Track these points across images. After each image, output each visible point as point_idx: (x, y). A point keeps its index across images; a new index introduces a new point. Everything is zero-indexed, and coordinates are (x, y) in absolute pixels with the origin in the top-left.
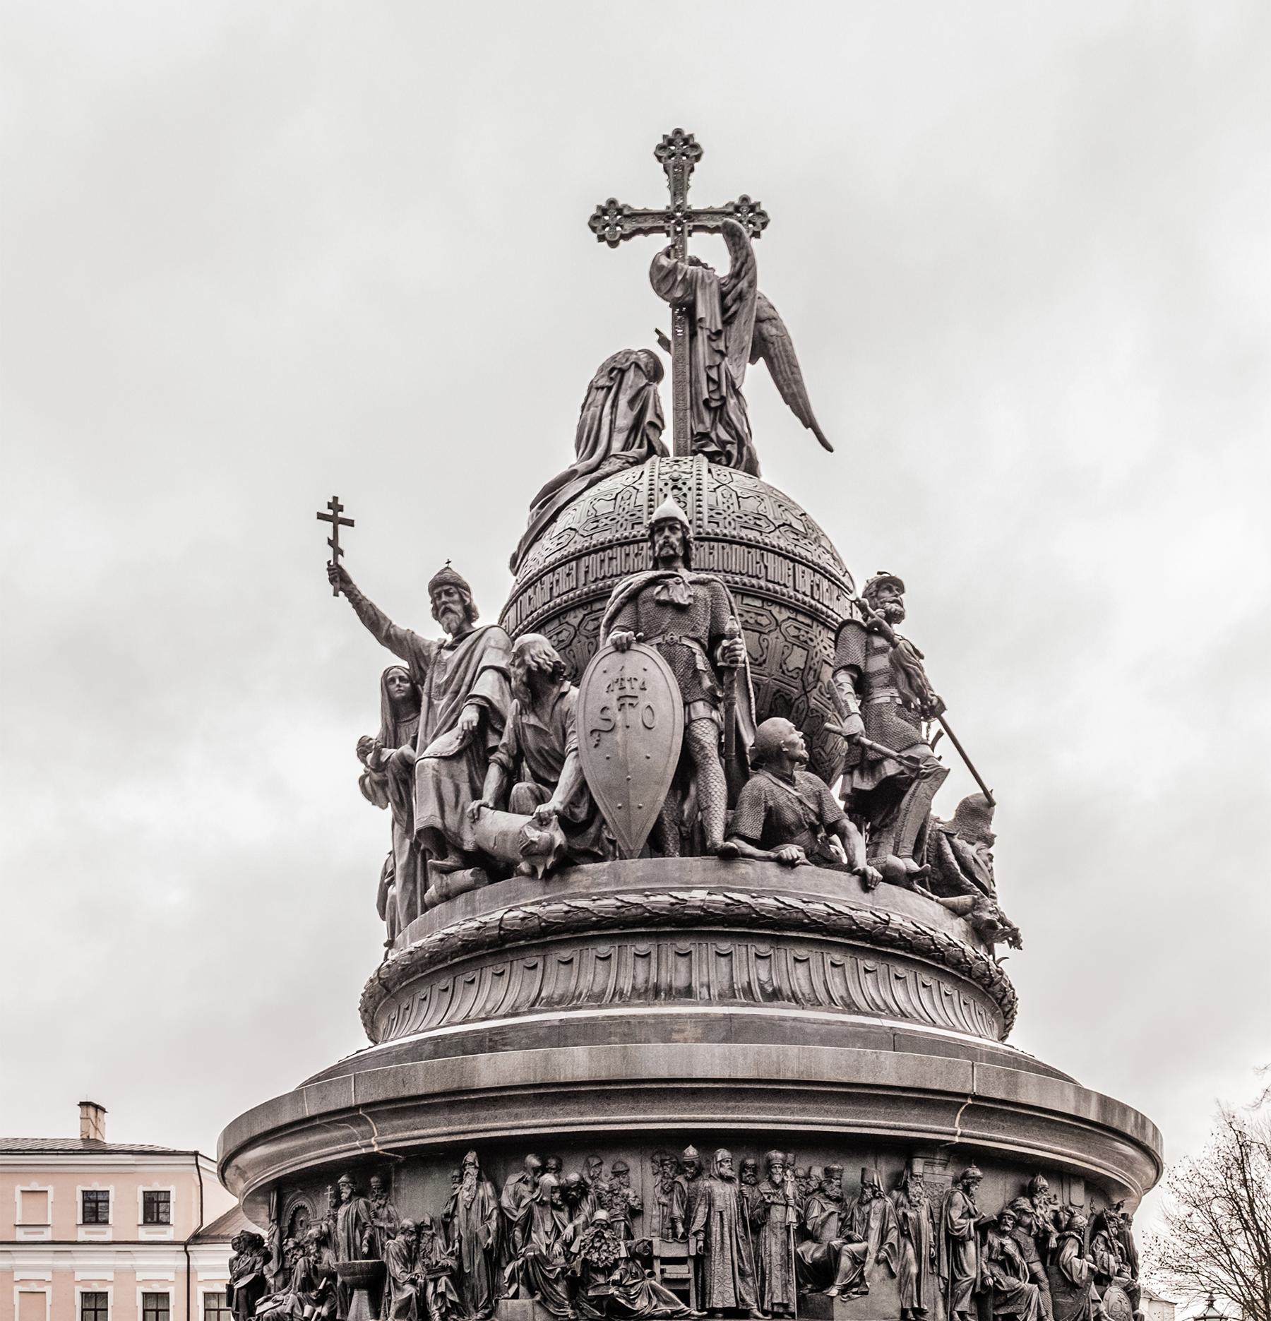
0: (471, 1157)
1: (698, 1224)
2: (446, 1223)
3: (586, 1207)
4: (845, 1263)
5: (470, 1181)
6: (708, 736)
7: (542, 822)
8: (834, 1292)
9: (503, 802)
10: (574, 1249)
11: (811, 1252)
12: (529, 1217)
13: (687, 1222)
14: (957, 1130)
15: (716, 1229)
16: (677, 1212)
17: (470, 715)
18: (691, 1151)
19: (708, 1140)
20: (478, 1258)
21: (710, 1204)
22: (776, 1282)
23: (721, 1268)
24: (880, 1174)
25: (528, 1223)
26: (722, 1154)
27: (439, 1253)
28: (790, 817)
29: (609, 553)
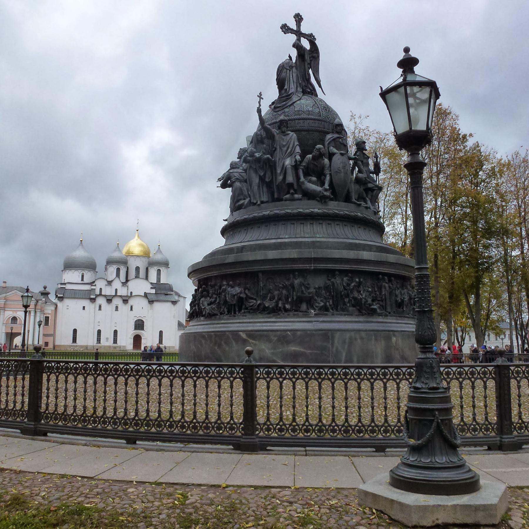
1: (384, 293)
7: (326, 190)
16: (376, 289)
17: (298, 158)
18: (381, 276)
19: (384, 274)
25: (352, 291)
26: (386, 277)
29: (315, 121)
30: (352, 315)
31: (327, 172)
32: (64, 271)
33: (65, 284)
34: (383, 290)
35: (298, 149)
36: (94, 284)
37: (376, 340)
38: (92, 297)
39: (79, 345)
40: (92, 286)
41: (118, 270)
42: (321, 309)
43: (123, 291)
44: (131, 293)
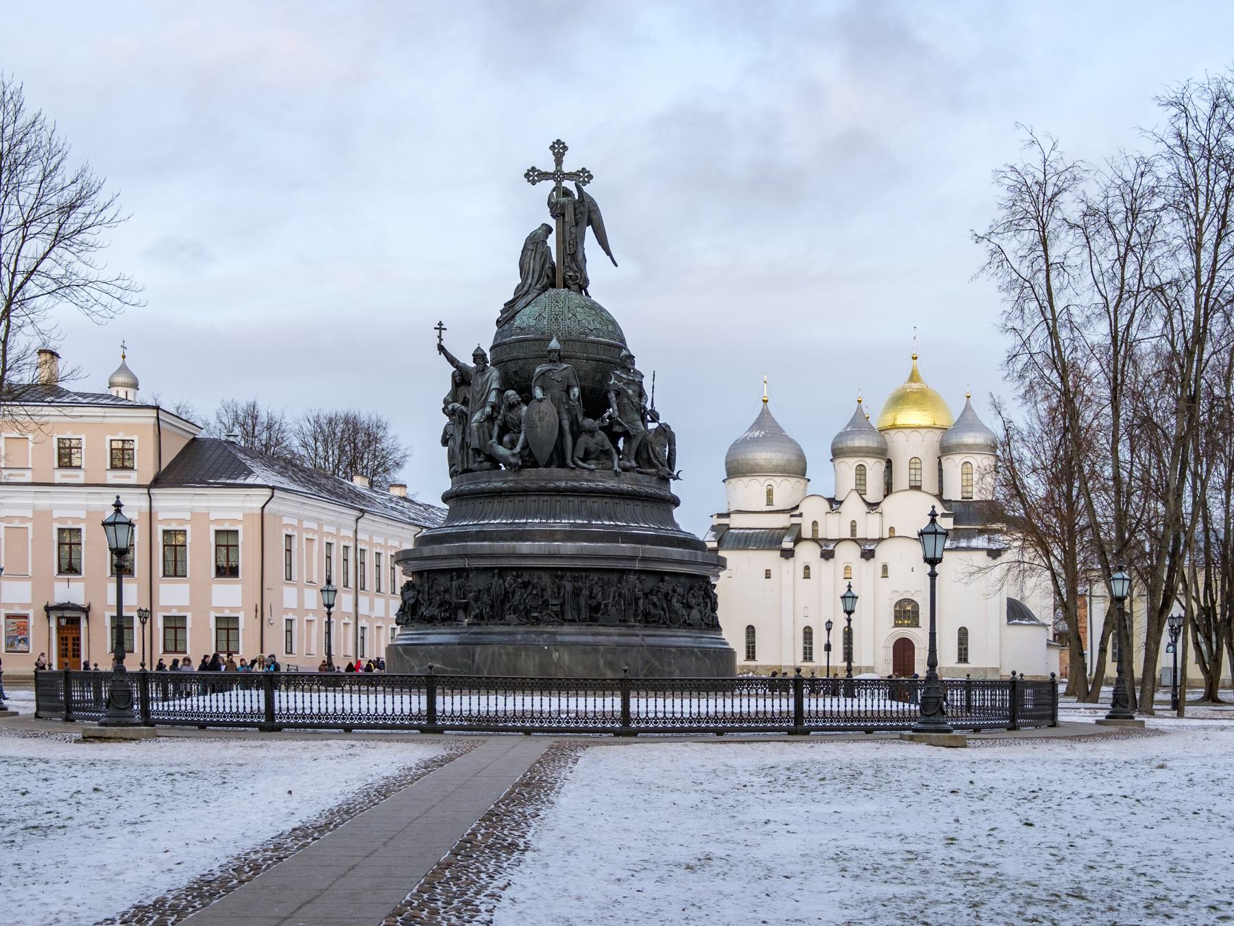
0: (496, 571)
1: (562, 594)
2: (488, 590)
3: (530, 588)
4: (602, 606)
5: (496, 578)
6: (566, 424)
7: (514, 455)
8: (599, 615)
9: (500, 443)
10: (527, 601)
11: (594, 603)
12: (514, 591)
13: (559, 593)
14: (638, 566)
15: (566, 596)
16: (556, 590)
20: (499, 601)
21: (565, 589)
22: (583, 612)
23: (568, 608)
24: (615, 577)
27: (485, 598)
28: (592, 449)
30: (509, 625)
31: (523, 427)
32: (727, 482)
33: (728, 515)
34: (563, 590)
35: (492, 398)
36: (797, 512)
37: (527, 655)
38: (787, 544)
39: (762, 666)
40: (792, 516)
41: (861, 471)
42: (476, 617)
43: (870, 527)
44: (892, 529)
